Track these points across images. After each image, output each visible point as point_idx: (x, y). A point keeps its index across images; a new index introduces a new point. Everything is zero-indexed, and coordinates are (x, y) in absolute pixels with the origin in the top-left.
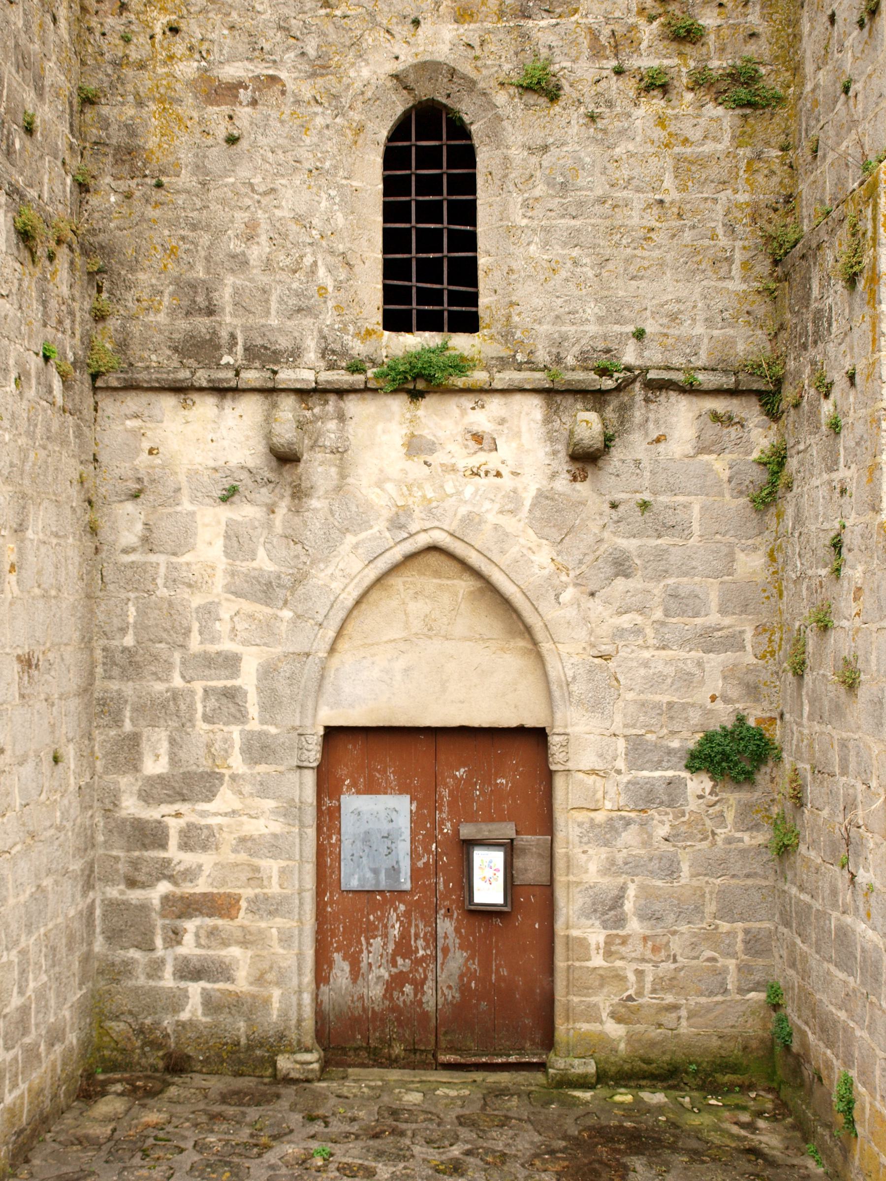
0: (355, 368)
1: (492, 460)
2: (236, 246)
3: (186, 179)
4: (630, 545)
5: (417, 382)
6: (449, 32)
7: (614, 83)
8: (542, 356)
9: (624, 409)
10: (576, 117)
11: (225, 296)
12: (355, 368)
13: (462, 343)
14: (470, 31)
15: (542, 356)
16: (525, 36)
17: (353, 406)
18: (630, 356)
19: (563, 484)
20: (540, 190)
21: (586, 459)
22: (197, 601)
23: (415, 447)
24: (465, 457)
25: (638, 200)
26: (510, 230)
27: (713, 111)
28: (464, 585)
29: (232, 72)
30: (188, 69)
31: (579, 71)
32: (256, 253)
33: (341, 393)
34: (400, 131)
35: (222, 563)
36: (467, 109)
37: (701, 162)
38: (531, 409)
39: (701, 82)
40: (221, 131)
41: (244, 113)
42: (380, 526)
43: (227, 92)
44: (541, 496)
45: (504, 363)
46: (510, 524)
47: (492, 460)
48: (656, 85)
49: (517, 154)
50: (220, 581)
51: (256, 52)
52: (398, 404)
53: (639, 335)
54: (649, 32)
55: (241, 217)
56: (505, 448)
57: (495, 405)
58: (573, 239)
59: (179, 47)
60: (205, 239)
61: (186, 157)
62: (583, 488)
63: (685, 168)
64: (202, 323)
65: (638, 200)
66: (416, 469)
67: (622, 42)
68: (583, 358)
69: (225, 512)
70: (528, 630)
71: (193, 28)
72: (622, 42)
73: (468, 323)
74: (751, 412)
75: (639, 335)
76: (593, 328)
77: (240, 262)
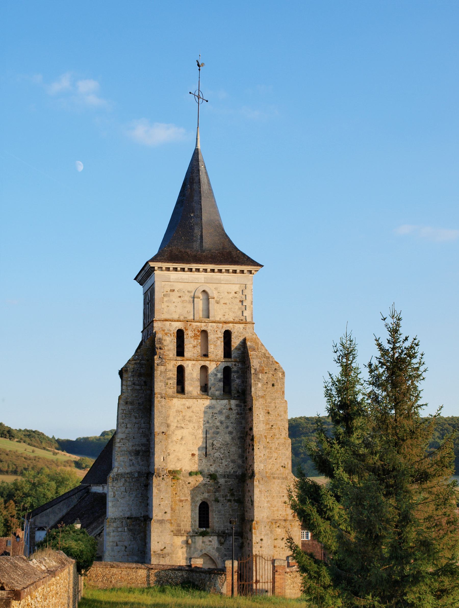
0: (196, 533)
1: (212, 544)
2: (183, 519)
3: (177, 511)
4: (226, 553)
5: (203, 534)
6: (207, 494)
7: (225, 501)
8: (217, 532)
9: (226, 538)
10: (221, 504)
11: (182, 525)
12: (196, 533)
13: (209, 530)
14: (209, 494)
15: (217, 532)
16: (215, 495)
17: (196, 537)
18: (226, 532)
19: (219, 546)
20: (217, 513)
21: (221, 543)
22: (179, 560)
23: (203, 542)
24: (208, 543)
25: (227, 514)
26: (214, 517)
27: (236, 504)
28: (208, 558)
29: (183, 499)
30: (178, 498)
31: (221, 499)
32: (185, 520)
33: (195, 536)
34: (200, 505)
35: (182, 556)
36: (208, 503)
37: (234, 509)
38: (216, 538)
39: (234, 500)
40: (181, 505)
41: (184, 503)
42: (199, 551)
43: (181, 501)
44: (217, 548)
45: (213, 532)
46: (213, 551)
47: (212, 544)
48: (229, 501)
49: (214, 508)
50: (181, 557)
51: (185, 496)
52: (201, 537)
53: (228, 529)
54: (229, 495)
55: (183, 516)
56: (213, 542)
57: (212, 537)
58: (220, 518)
59: (177, 496)
60: (179, 518)
61: (177, 508)
62: (221, 547)
63: (233, 510)
64: (179, 528)
65: (227, 514)
66: (203, 545)
67: (226, 496)
68: (221, 532)
69: (182, 550)
70: (215, 563)
71: (178, 493)
72: (226, 496)
73: (207, 526)
74: (239, 538)
75: (228, 529)
76: (222, 528)
77: (183, 521)
